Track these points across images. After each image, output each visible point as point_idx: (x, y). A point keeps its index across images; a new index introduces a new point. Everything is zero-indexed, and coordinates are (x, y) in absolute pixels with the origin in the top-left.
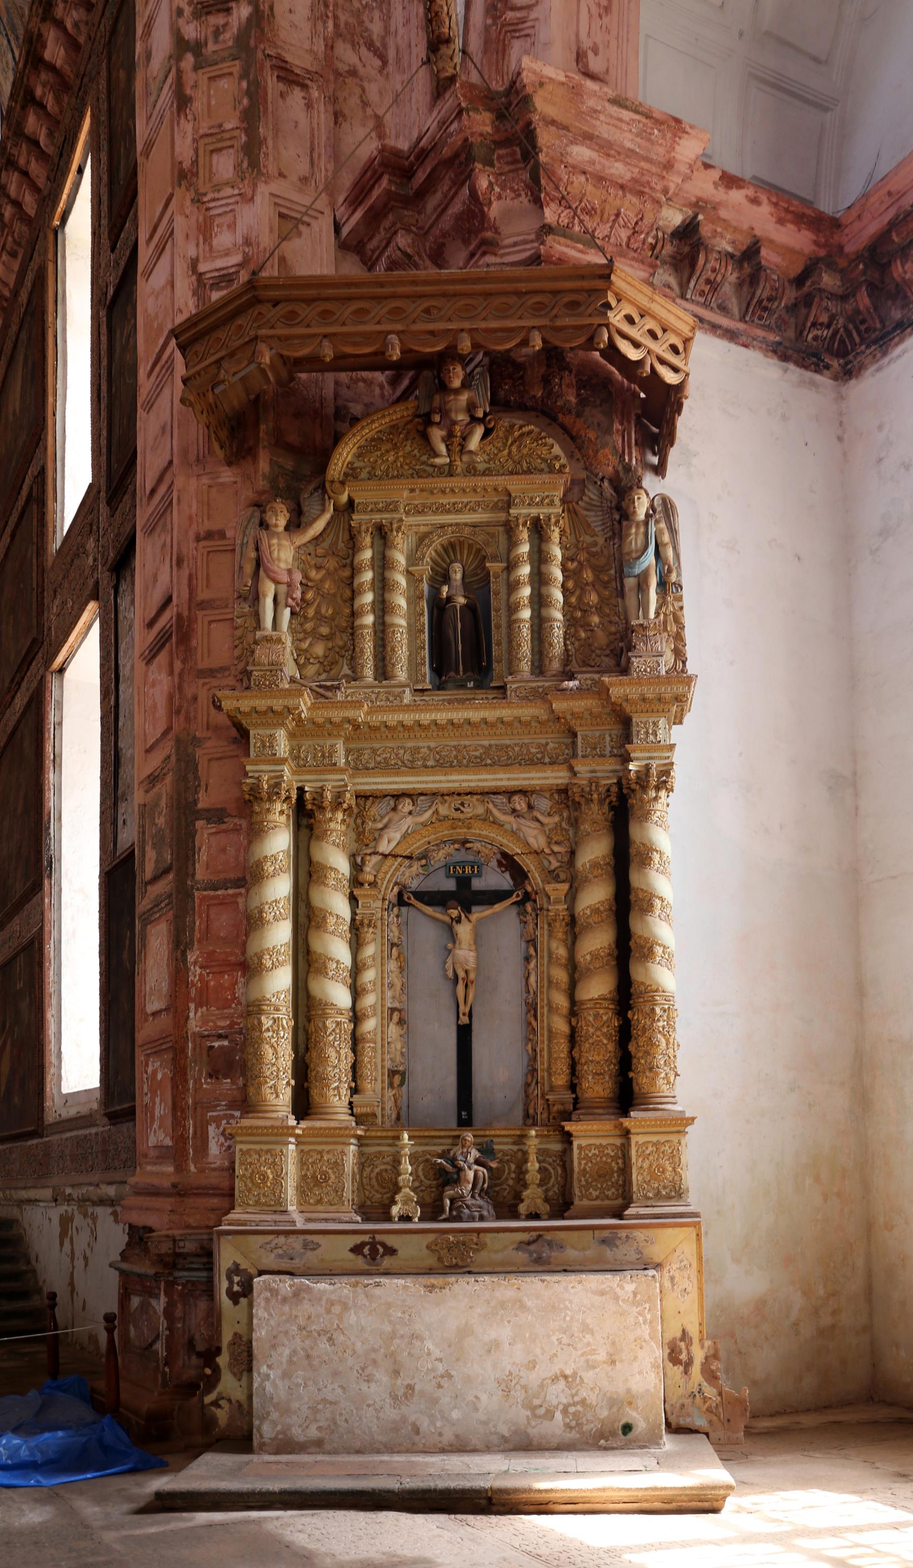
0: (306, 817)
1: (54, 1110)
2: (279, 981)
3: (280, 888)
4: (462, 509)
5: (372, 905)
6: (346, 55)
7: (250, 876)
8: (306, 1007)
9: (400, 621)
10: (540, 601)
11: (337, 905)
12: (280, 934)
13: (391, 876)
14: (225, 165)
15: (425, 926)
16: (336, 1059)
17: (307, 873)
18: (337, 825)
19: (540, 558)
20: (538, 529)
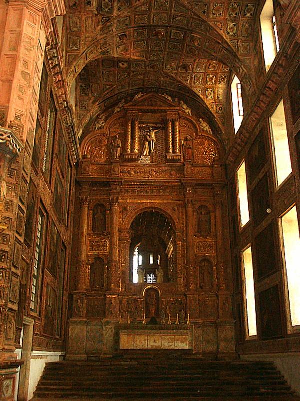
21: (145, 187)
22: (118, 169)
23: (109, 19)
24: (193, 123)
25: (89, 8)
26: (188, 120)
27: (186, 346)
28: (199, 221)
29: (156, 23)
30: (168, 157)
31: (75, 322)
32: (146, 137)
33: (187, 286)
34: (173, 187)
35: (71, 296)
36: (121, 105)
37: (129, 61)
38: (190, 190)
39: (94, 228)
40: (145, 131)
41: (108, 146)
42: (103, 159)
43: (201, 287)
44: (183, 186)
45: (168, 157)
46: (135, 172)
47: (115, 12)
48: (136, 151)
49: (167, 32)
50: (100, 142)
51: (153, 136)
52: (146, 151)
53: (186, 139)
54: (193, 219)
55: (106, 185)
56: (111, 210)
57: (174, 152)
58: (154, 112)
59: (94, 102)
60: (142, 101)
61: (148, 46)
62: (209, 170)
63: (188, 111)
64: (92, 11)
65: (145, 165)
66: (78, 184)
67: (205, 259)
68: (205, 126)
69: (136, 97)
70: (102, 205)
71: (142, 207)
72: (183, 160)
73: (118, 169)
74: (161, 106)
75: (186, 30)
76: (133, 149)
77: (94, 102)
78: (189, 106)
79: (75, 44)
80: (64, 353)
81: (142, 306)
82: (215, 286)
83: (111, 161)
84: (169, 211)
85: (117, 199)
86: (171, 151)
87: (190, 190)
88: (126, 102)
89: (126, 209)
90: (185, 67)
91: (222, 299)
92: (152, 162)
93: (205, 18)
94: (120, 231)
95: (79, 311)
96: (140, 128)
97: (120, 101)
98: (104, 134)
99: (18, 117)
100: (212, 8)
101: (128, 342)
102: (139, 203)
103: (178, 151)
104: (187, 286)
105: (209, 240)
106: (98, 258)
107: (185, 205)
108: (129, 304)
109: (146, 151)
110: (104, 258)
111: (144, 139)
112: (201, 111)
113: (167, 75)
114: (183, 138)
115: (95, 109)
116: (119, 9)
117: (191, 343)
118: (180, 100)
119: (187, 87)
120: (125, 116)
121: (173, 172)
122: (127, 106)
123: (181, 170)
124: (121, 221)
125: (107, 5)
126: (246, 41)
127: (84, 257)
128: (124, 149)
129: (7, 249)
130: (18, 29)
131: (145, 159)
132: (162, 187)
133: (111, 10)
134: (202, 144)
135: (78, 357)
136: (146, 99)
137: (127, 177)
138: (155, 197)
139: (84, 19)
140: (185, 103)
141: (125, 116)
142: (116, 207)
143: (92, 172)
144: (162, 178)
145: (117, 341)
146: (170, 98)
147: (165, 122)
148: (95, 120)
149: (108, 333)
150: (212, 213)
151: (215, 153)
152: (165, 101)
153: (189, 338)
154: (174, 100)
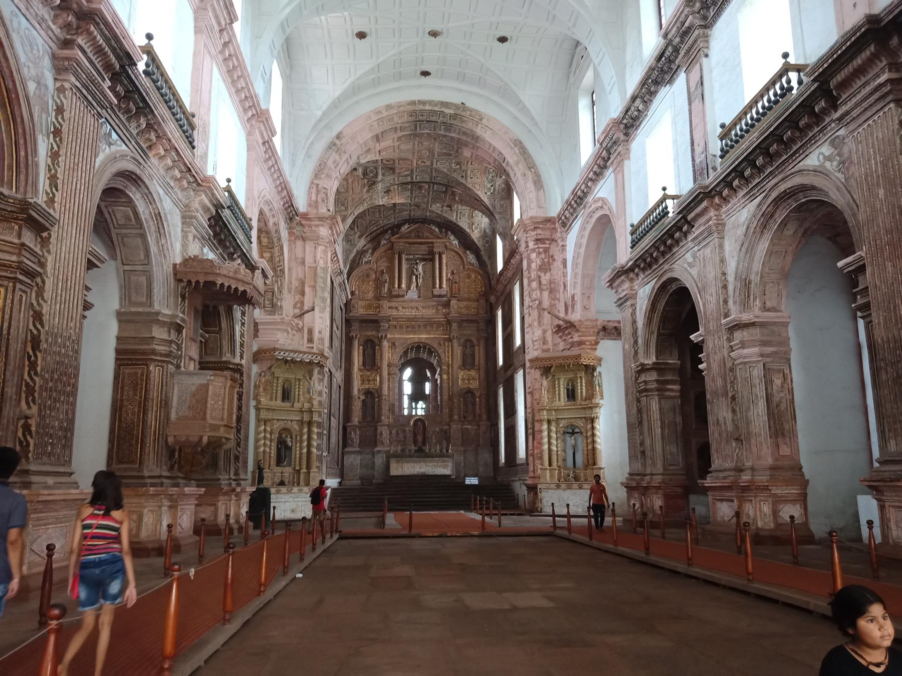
0: (549, 422)
1: (518, 462)
2: (546, 447)
3: (545, 433)
4: (571, 376)
5: (559, 435)
6: (553, 302)
7: (541, 431)
8: (550, 450)
9: (562, 393)
10: (581, 389)
11: (554, 435)
12: (546, 440)
13: (562, 430)
14: (536, 323)
15: (568, 437)
16: (554, 458)
17: (549, 431)
18: (553, 424)
19: (581, 382)
20: (581, 378)
21: (412, 324)
22: (385, 304)
23: (374, 183)
24: (459, 255)
25: (355, 173)
26: (455, 252)
27: (447, 471)
28: (464, 355)
29: (418, 180)
30: (435, 293)
31: (349, 452)
32: (413, 271)
33: (451, 416)
34: (439, 324)
35: (345, 428)
36: (387, 237)
37: (394, 204)
38: (455, 326)
39: (364, 364)
40: (413, 263)
41: (377, 279)
42: (371, 295)
43: (465, 417)
44: (449, 322)
45: (435, 293)
46: (403, 308)
47: (380, 177)
48: (403, 286)
49: (429, 187)
50: (368, 276)
51: (420, 268)
52: (414, 286)
53: (453, 273)
54: (458, 351)
55: (373, 322)
56: (380, 345)
57: (440, 287)
58: (421, 243)
59: (360, 237)
60: (409, 232)
61: (412, 193)
62: (475, 304)
63: (456, 242)
64: (358, 176)
65: (411, 301)
66: (348, 322)
67: (469, 392)
68: (471, 258)
69: (403, 229)
70: (372, 341)
71: (409, 342)
72: (449, 295)
73: (385, 304)
74: (427, 238)
75: (447, 186)
76: (399, 286)
77: (360, 237)
78: (457, 237)
79: (343, 205)
80: (338, 480)
81: (410, 435)
82: (477, 417)
83: (378, 297)
84: (435, 345)
85: (386, 336)
86: (438, 286)
87: (455, 326)
88: (393, 234)
89: (394, 344)
90: (450, 206)
91: (483, 428)
92: (419, 297)
93: (464, 182)
94: (389, 365)
95: (352, 442)
96: (407, 260)
97: (385, 232)
98: (371, 269)
99: (320, 332)
100: (469, 173)
101: (397, 469)
102: (407, 339)
103: (444, 286)
104: (451, 416)
105: (473, 373)
106: (368, 393)
107: (450, 340)
108: (397, 433)
109: (414, 286)
110: (374, 391)
111: (411, 273)
112: (467, 242)
113: (432, 212)
114: (450, 271)
115: (361, 243)
116: (383, 175)
117: (452, 470)
118: (446, 232)
119: (451, 222)
120: (391, 248)
121: (440, 307)
122: (393, 239)
123: (447, 305)
124: (388, 355)
125: (371, 172)
126: (502, 199)
127: (355, 392)
128: (392, 284)
129: (320, 420)
130: (314, 265)
131: (413, 294)
132: (429, 324)
133: (376, 175)
134: (469, 277)
135: (354, 482)
136: (412, 231)
137: (394, 313)
138: (421, 334)
139: (350, 181)
140: (453, 233)
141: (391, 248)
142: (385, 343)
143: (360, 310)
144: (429, 313)
145: (387, 467)
146: (437, 230)
147: (432, 253)
148: (361, 253)
149: (379, 460)
150: (476, 348)
151: (481, 287)
152: (432, 232)
153: (450, 464)
154: (441, 232)
